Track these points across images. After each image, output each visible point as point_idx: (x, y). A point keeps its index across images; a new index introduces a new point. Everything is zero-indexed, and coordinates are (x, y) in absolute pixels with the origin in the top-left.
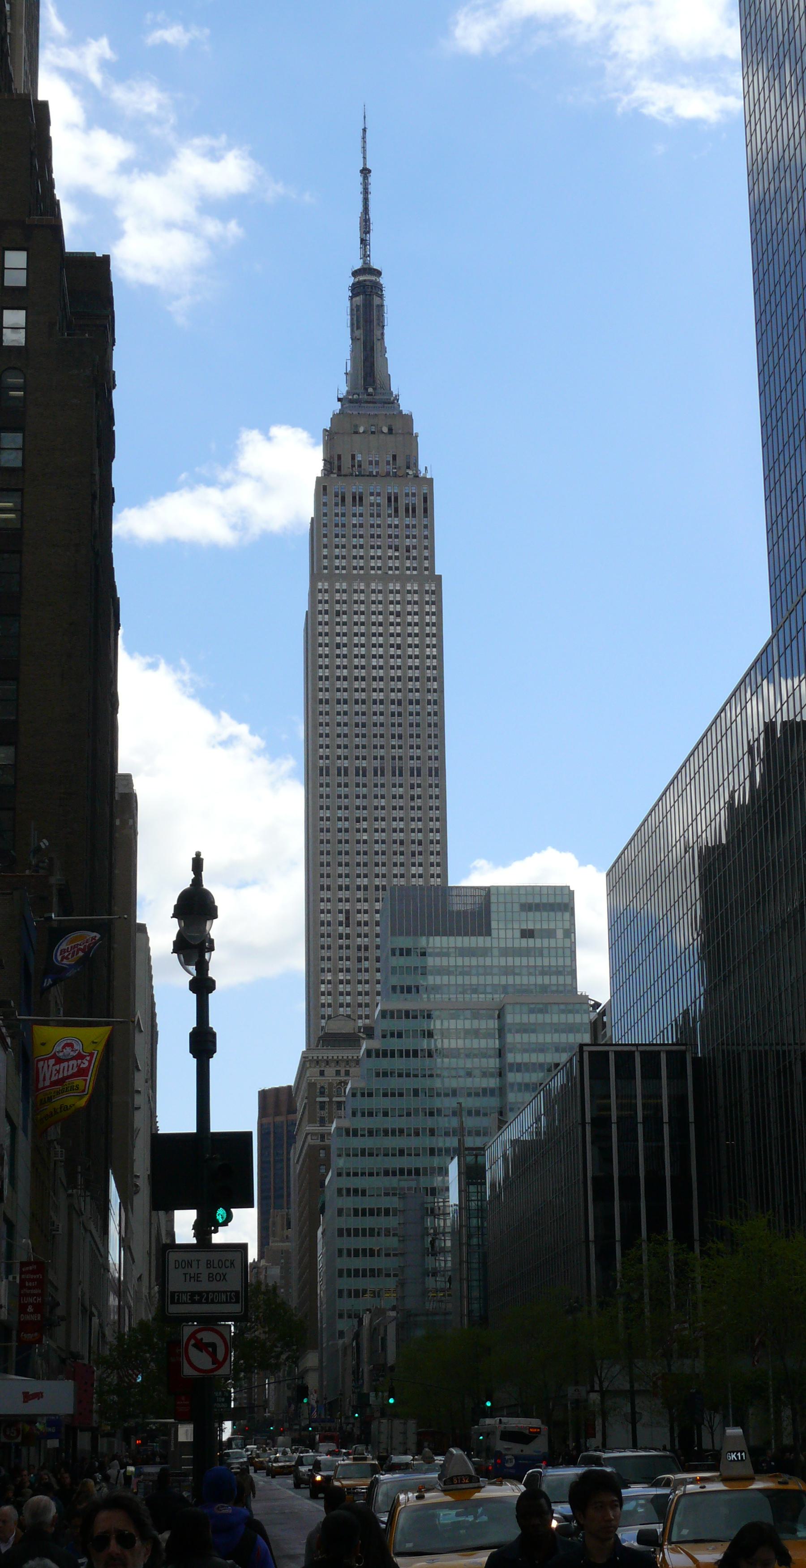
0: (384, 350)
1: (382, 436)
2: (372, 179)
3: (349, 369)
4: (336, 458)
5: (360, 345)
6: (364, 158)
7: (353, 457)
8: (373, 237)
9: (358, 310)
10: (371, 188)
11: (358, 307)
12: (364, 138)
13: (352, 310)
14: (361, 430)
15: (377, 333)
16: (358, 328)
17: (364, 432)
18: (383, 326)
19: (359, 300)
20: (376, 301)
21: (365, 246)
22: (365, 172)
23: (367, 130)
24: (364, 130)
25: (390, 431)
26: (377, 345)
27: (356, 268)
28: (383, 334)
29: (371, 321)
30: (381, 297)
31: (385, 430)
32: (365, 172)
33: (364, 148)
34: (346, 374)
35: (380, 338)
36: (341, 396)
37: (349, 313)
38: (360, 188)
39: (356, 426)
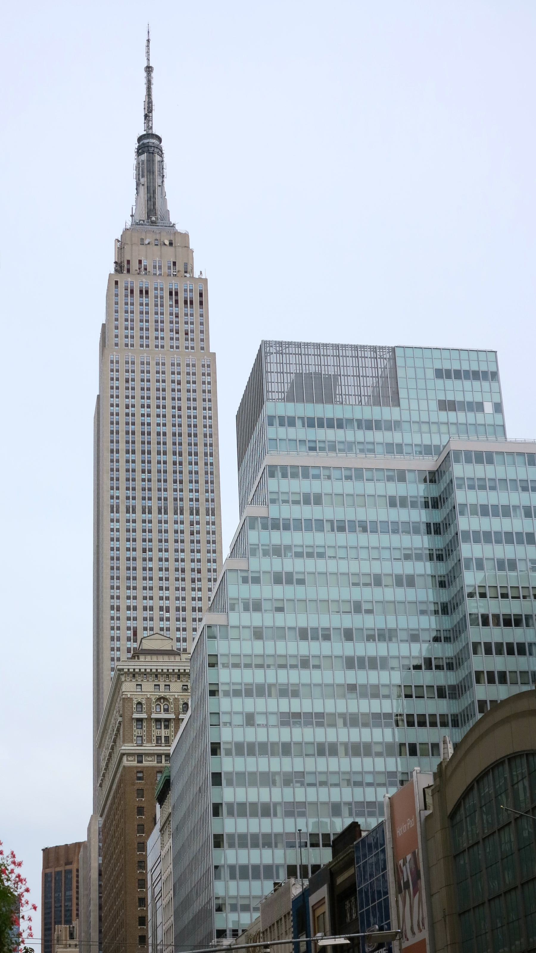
0: (163, 195)
1: (164, 248)
2: (153, 74)
3: (134, 212)
4: (126, 262)
5: (143, 190)
6: (148, 60)
7: (140, 262)
8: (155, 114)
9: (143, 164)
10: (153, 81)
11: (143, 161)
12: (148, 46)
13: (138, 164)
14: (147, 242)
15: (158, 181)
16: (143, 176)
17: (149, 244)
18: (163, 176)
19: (144, 157)
20: (157, 158)
21: (149, 121)
22: (149, 69)
23: (150, 42)
24: (148, 41)
25: (171, 244)
26: (158, 190)
27: (141, 134)
28: (163, 181)
29: (153, 173)
30: (161, 155)
31: (167, 242)
32: (149, 69)
33: (148, 52)
34: (132, 216)
35: (160, 184)
36: (128, 227)
37: (135, 169)
38: (144, 81)
39: (142, 240)
